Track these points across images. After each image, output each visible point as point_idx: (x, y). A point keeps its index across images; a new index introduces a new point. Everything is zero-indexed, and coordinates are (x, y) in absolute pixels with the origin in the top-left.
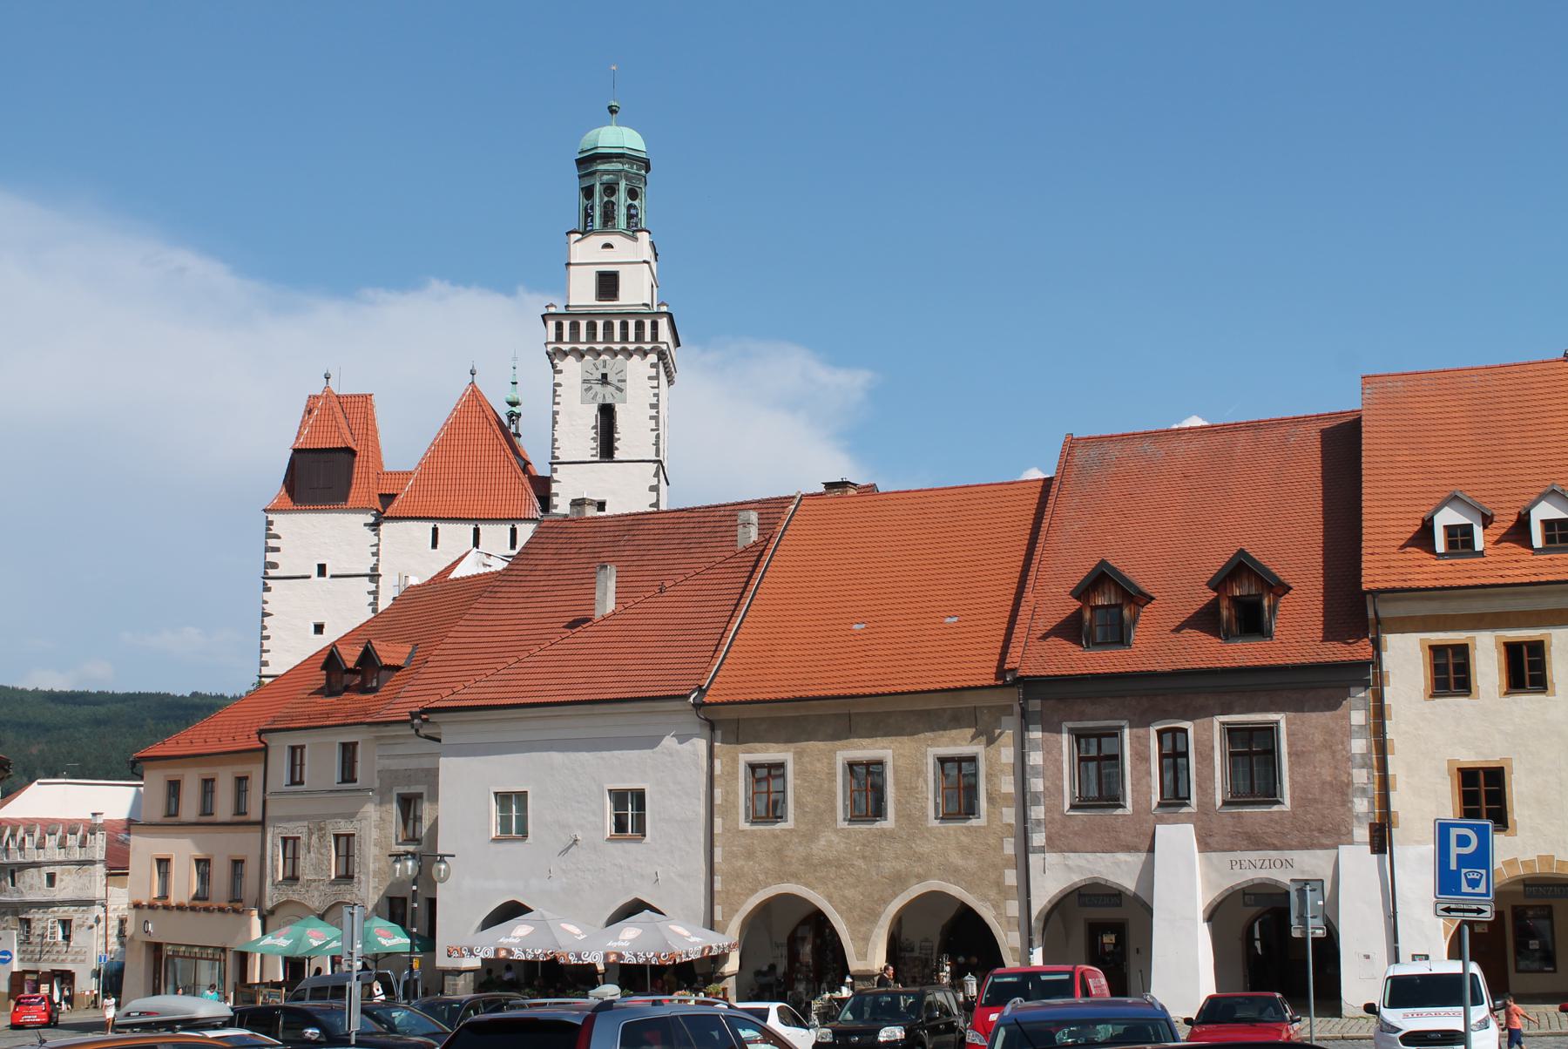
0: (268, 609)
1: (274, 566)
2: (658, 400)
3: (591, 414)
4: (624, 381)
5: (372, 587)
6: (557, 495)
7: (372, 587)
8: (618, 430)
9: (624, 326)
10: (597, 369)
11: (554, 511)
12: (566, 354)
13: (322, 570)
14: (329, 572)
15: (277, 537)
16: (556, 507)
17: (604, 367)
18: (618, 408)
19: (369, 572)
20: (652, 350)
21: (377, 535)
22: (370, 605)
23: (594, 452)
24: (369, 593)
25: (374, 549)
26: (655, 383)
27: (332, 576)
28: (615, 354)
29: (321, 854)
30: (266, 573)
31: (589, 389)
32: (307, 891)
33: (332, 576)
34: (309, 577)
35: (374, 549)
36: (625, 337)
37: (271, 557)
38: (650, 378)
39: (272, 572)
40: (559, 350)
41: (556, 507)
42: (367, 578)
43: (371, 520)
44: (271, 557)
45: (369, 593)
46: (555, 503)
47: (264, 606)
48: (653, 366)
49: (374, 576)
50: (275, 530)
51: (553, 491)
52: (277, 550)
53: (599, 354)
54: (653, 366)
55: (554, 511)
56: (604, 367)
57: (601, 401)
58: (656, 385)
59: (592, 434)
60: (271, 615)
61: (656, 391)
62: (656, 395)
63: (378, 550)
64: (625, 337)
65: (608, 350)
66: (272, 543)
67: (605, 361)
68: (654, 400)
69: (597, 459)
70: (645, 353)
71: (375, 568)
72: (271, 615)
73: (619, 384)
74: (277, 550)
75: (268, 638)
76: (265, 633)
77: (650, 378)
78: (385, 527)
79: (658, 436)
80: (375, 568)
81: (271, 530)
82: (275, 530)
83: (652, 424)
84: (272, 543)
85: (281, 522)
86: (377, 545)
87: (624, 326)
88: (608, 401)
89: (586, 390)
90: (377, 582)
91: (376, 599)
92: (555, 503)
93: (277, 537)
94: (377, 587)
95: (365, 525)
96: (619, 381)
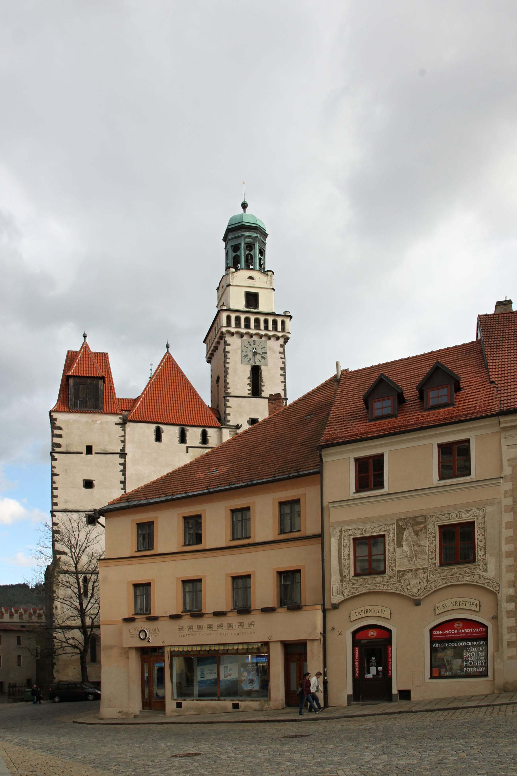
0: (56, 471)
1: (59, 445)
2: (285, 366)
3: (247, 370)
4: (266, 353)
5: (122, 461)
6: (229, 414)
7: (122, 461)
8: (263, 381)
9: (266, 322)
10: (250, 345)
11: (228, 423)
12: (232, 334)
13: (89, 450)
14: (94, 451)
15: (60, 428)
16: (229, 421)
17: (254, 344)
18: (263, 368)
19: (119, 451)
20: (282, 336)
21: (124, 430)
22: (121, 471)
23: (249, 392)
24: (120, 464)
25: (123, 439)
26: (283, 356)
27: (97, 453)
28: (261, 337)
29: (420, 546)
30: (53, 449)
31: (246, 356)
32: (399, 581)
33: (97, 453)
34: (82, 453)
35: (123, 439)
36: (266, 328)
37: (57, 440)
38: (280, 353)
39: (57, 449)
40: (228, 332)
41: (229, 421)
42: (118, 455)
43: (120, 421)
44: (57, 440)
45: (120, 464)
46: (228, 419)
47: (54, 469)
48: (282, 346)
49: (123, 454)
50: (58, 424)
51: (227, 412)
52: (60, 436)
53: (251, 336)
54: (282, 346)
55: (228, 423)
56: (254, 344)
57: (253, 364)
58: (283, 357)
59: (248, 381)
60: (58, 475)
61: (283, 360)
62: (284, 363)
63: (125, 439)
64: (266, 328)
65: (257, 334)
66: (57, 432)
67: (254, 341)
68: (283, 366)
69: (250, 396)
70: (278, 338)
71: (123, 450)
72: (58, 475)
73: (263, 355)
74: (60, 436)
75: (56, 489)
76: (54, 486)
77: (280, 353)
78: (130, 426)
79: (285, 386)
80: (123, 450)
81: (56, 424)
82: (58, 424)
83: (282, 378)
84: (57, 432)
85: (62, 418)
86: (124, 436)
87: (266, 322)
88: (257, 363)
89: (244, 356)
90: (125, 458)
91: (125, 468)
92: (228, 419)
93: (60, 428)
94: (125, 461)
95: (116, 424)
96: (263, 353)
